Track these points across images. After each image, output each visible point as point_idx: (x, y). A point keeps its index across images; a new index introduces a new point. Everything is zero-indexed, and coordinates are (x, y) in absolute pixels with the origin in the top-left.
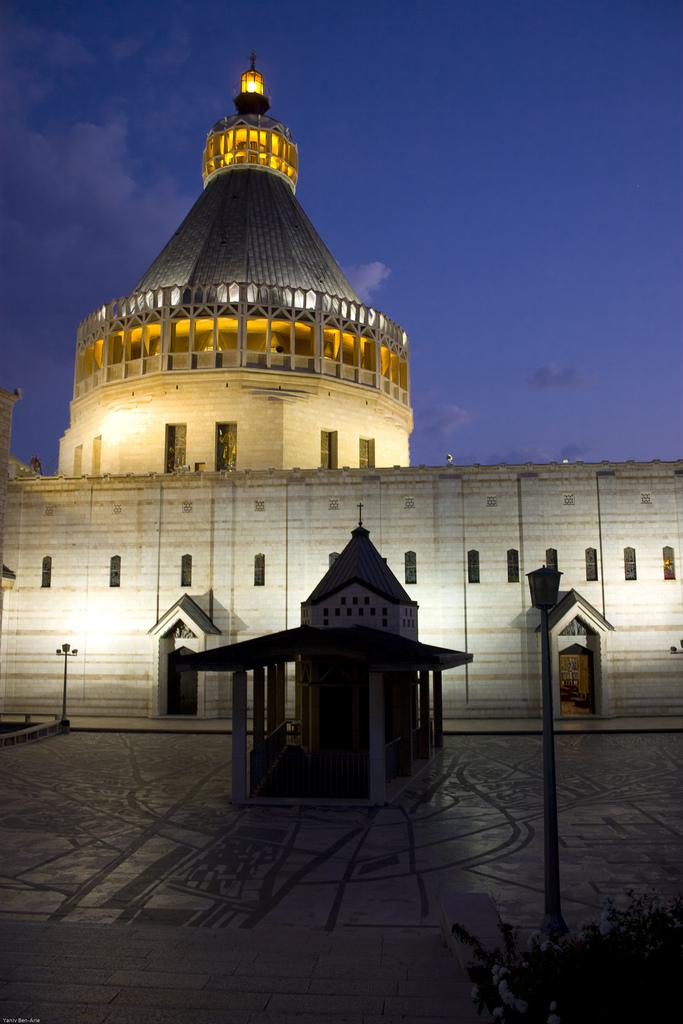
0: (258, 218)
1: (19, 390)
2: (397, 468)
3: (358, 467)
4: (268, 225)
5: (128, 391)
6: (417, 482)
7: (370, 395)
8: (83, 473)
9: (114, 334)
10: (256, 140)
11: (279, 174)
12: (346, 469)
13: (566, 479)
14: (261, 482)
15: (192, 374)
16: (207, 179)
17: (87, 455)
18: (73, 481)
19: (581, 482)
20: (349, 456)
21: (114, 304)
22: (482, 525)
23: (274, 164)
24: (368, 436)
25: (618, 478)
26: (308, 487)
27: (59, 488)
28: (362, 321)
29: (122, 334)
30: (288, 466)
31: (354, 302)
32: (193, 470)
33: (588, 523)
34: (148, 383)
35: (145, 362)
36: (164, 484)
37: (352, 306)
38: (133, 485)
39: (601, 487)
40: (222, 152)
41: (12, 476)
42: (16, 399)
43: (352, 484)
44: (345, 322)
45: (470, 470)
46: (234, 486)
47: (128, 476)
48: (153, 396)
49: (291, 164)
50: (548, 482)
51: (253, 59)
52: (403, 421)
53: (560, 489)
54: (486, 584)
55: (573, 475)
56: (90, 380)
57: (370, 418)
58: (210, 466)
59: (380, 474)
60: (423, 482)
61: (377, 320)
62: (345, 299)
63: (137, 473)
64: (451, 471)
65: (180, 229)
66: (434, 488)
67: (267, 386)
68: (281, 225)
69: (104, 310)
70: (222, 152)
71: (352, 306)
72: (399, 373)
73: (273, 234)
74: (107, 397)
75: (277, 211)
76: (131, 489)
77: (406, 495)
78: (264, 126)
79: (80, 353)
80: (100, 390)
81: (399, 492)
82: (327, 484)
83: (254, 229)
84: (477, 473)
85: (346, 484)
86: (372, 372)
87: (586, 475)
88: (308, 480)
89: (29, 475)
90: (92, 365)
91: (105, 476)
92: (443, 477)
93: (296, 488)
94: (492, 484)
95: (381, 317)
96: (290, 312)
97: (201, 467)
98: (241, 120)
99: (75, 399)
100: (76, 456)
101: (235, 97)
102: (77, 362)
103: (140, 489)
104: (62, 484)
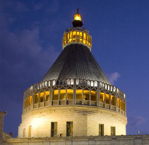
0: (80, 59)
1: (6, 112)
2: (122, 135)
3: (110, 135)
4: (83, 61)
5: (39, 112)
6: (128, 140)
7: (114, 113)
8: (26, 137)
9: (35, 94)
10: (79, 35)
11: (86, 45)
12: (107, 136)
14: (81, 140)
15: (66, 106)
16: (64, 47)
17: (27, 131)
18: (22, 139)
20: (107, 132)
21: (35, 85)
23: (84, 42)
24: (113, 126)
26: (95, 141)
27: (18, 142)
28: (111, 90)
29: (37, 94)
30: (89, 135)
31: (109, 85)
32: (59, 136)
34: (46, 109)
35: (45, 103)
36: (51, 140)
37: (108, 86)
38: (41, 141)
40: (68, 39)
41: (4, 138)
42: (5, 114)
43: (108, 140)
44: (106, 91)
45: (145, 136)
46: (72, 141)
47: (39, 138)
48: (47, 113)
49: (90, 42)
51: (78, 10)
52: (124, 121)
56: (28, 108)
57: (114, 120)
58: (65, 135)
59: (117, 138)
60: (130, 140)
61: (116, 90)
62: (106, 84)
63: (42, 137)
64: (139, 136)
65: (55, 62)
66: (134, 142)
67: (82, 110)
68: (86, 60)
69: (32, 87)
70: (68, 39)
71: (108, 86)
72: (123, 106)
73: (84, 64)
74: (33, 114)
75: (85, 57)
76: (40, 142)
78: (81, 30)
79: (25, 100)
80: (31, 112)
81: (123, 143)
82: (100, 140)
83: (78, 62)
84: (147, 137)
86: (114, 106)
88: (95, 139)
89: (8, 137)
90: (28, 104)
91: (33, 138)
92: (136, 138)
93: (91, 142)
95: (117, 89)
96: (89, 87)
97: (62, 135)
98: (74, 29)
99: (23, 114)
100: (23, 132)
101: (72, 22)
102: (24, 103)
103: (43, 142)
104: (19, 140)
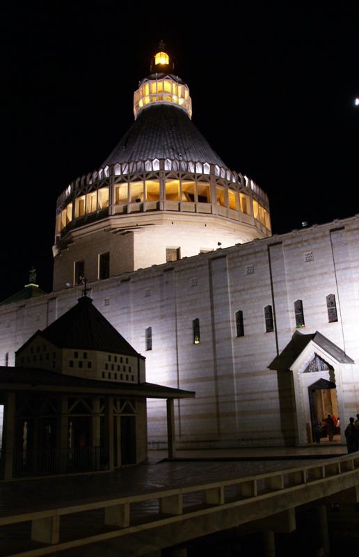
13: (306, 241)
19: (318, 241)
22: (244, 290)
25: (348, 231)
33: (326, 273)
39: (334, 241)
50: (292, 247)
53: (302, 250)
54: (249, 336)
55: (312, 236)
77: (191, 277)
81: (187, 276)
82: (143, 279)
84: (238, 251)
85: (154, 277)
87: (321, 234)
94: (250, 257)
